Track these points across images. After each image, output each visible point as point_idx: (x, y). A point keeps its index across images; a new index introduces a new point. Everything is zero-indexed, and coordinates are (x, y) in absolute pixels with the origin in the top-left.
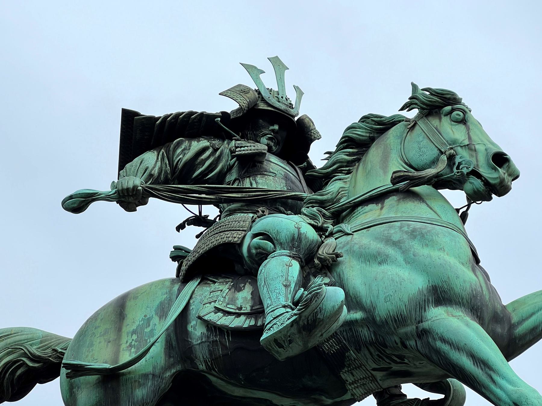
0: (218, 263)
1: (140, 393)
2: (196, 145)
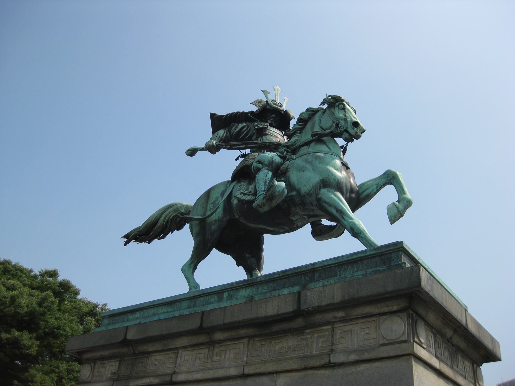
0: (244, 174)
1: (213, 227)
2: (240, 126)
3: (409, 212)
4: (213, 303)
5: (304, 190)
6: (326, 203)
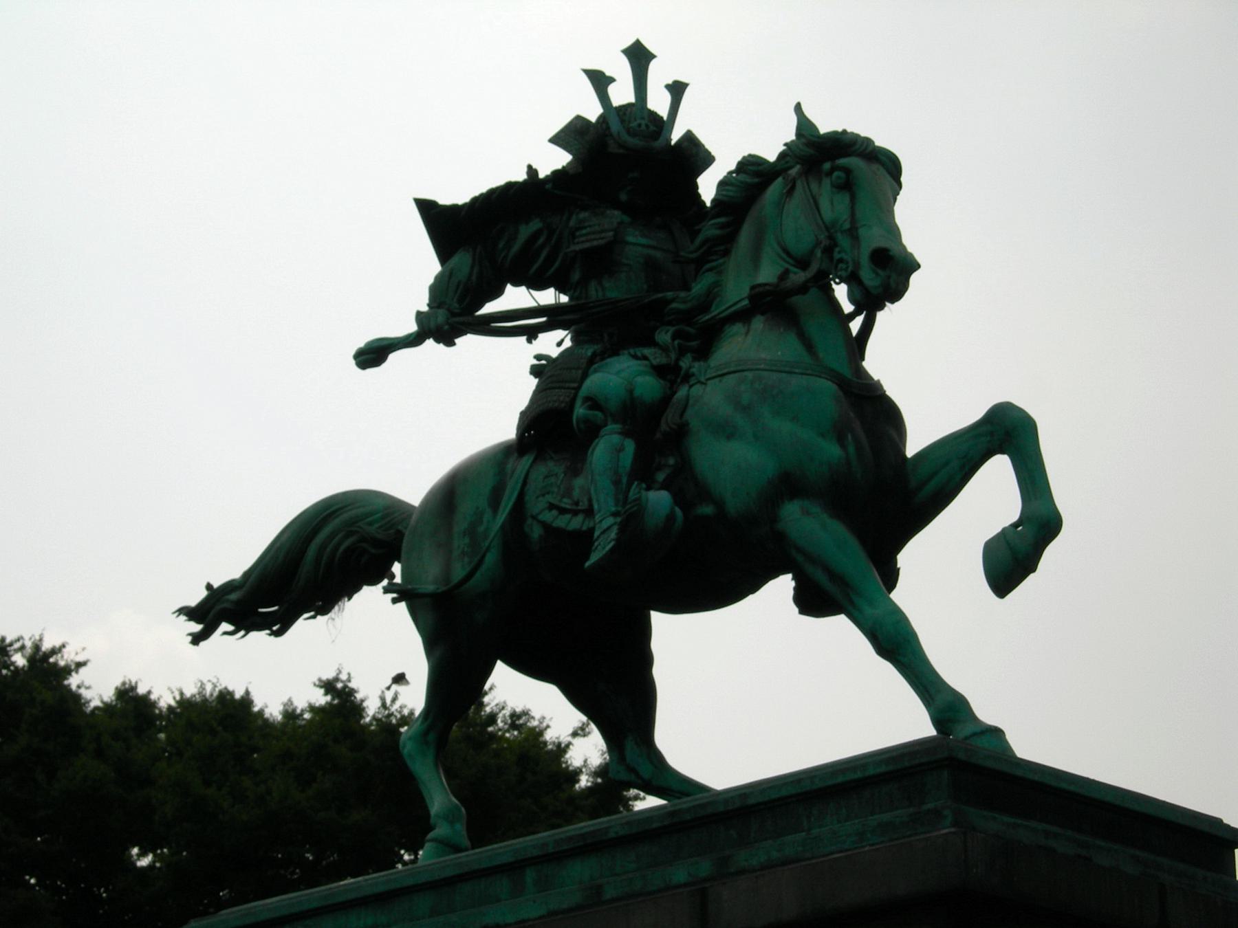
2: (525, 231)
3: (1052, 554)
4: (498, 900)
5: (734, 504)
6: (799, 550)
